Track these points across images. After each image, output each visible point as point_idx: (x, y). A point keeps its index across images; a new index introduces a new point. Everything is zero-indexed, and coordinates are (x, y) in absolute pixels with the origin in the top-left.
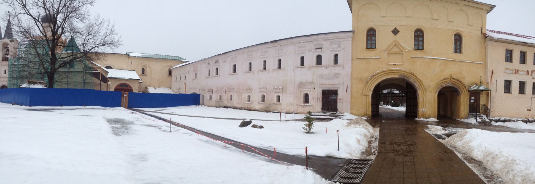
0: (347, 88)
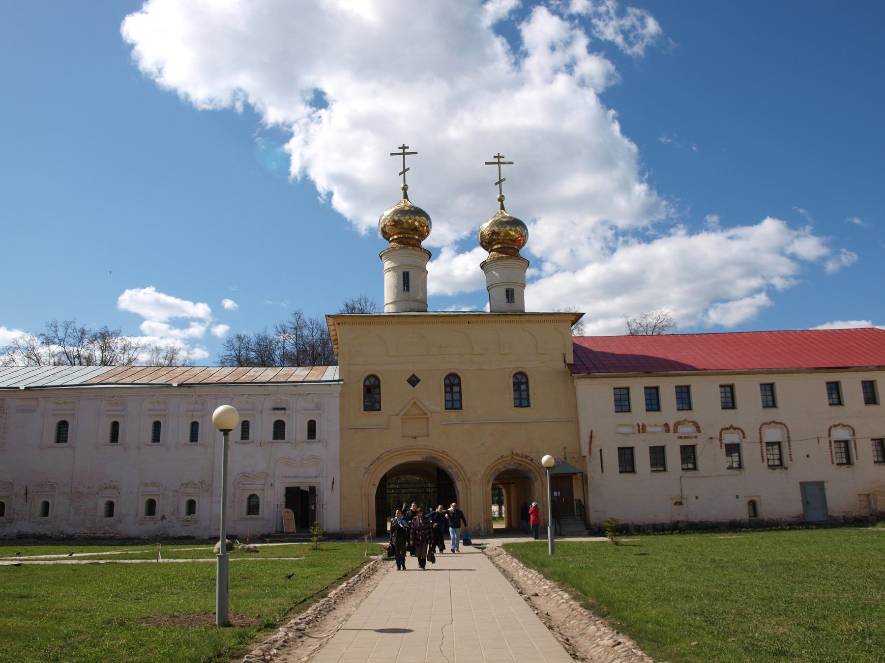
0: (333, 483)
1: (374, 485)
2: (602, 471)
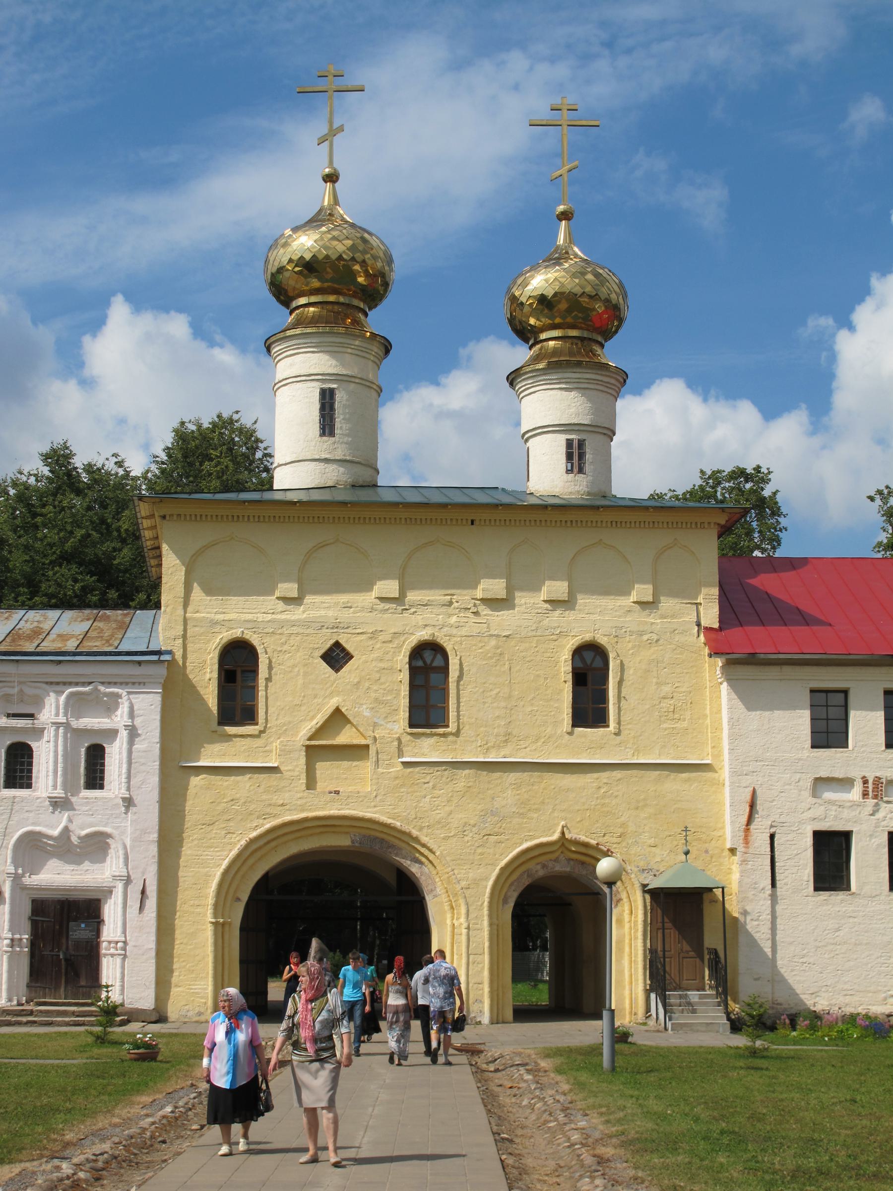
1: (238, 899)
2: (774, 884)
